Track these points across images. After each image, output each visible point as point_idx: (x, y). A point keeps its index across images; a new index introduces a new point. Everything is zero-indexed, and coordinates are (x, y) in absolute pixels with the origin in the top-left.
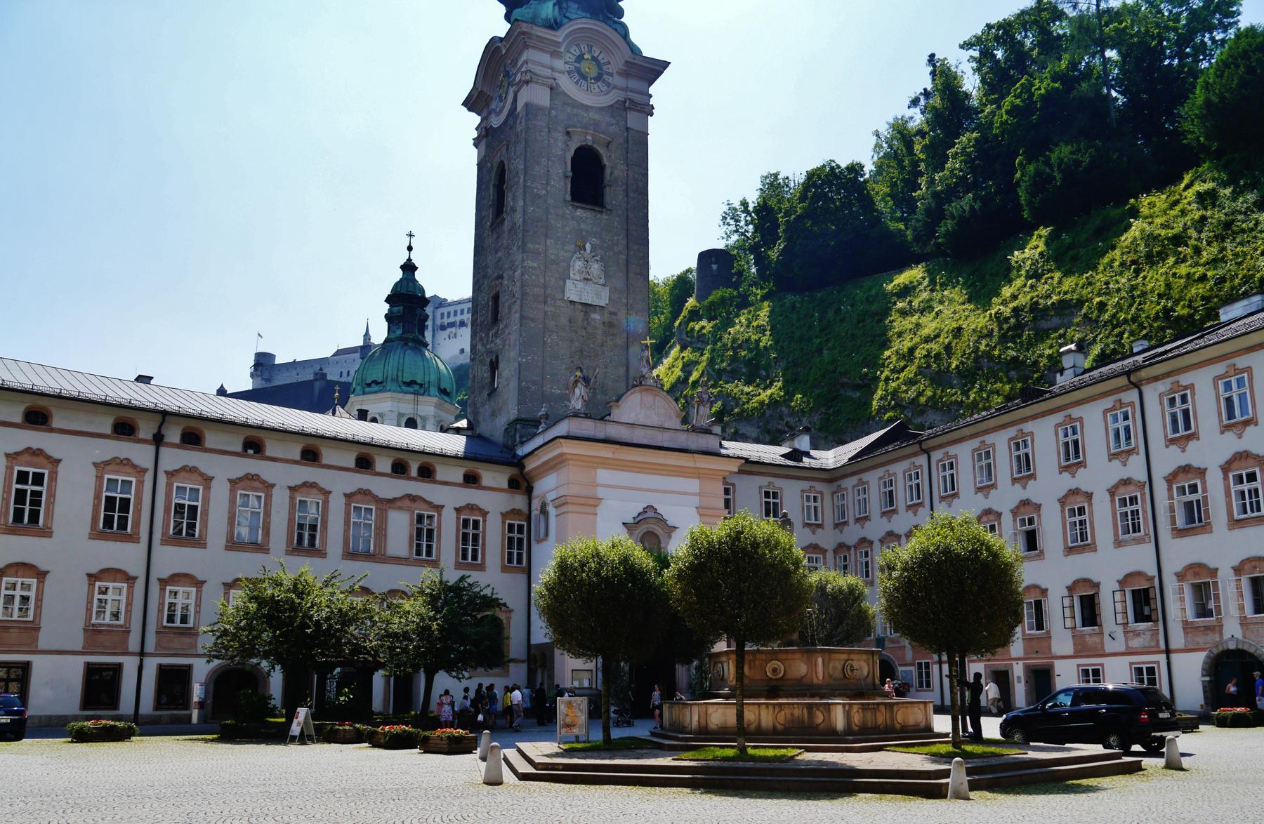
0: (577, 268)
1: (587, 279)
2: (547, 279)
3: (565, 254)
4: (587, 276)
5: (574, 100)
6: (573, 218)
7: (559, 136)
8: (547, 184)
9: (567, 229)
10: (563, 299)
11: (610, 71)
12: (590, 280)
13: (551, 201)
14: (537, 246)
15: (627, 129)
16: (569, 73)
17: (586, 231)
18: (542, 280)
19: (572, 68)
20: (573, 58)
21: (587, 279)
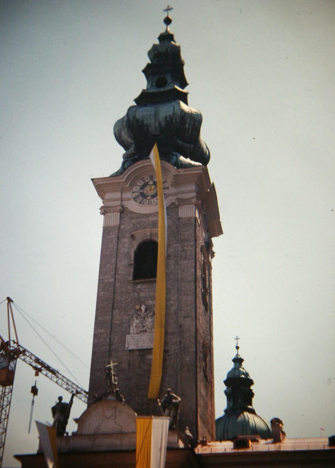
0: (135, 324)
1: (143, 331)
2: (112, 339)
3: (127, 318)
4: (142, 329)
5: (138, 214)
6: (134, 291)
7: (126, 240)
8: (115, 274)
9: (129, 300)
10: (124, 350)
11: (167, 186)
12: (146, 331)
13: (118, 285)
14: (105, 317)
15: (179, 219)
16: (135, 199)
17: (143, 297)
18: (108, 341)
19: (137, 194)
20: (139, 188)
21: (143, 331)
